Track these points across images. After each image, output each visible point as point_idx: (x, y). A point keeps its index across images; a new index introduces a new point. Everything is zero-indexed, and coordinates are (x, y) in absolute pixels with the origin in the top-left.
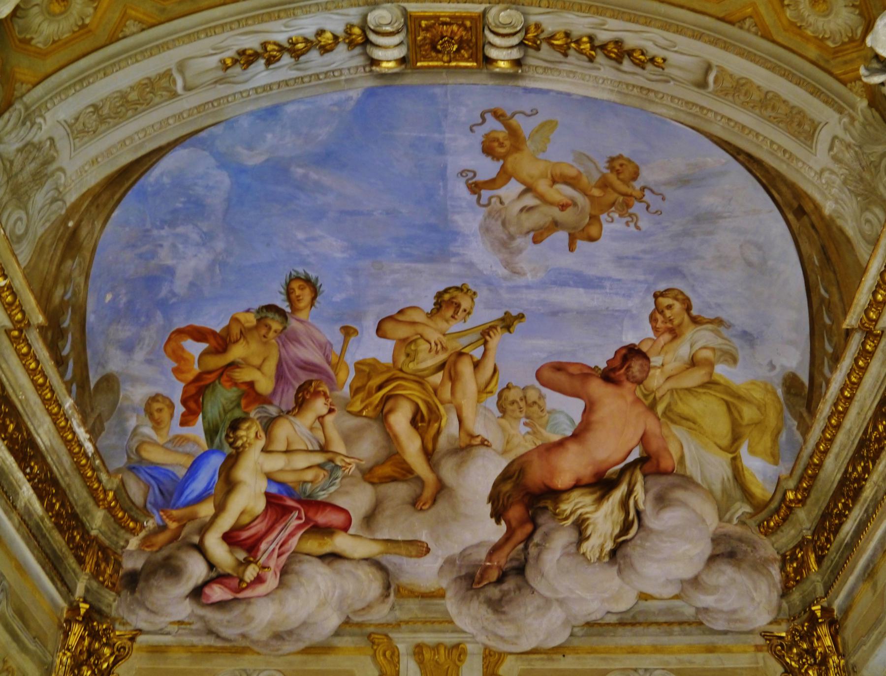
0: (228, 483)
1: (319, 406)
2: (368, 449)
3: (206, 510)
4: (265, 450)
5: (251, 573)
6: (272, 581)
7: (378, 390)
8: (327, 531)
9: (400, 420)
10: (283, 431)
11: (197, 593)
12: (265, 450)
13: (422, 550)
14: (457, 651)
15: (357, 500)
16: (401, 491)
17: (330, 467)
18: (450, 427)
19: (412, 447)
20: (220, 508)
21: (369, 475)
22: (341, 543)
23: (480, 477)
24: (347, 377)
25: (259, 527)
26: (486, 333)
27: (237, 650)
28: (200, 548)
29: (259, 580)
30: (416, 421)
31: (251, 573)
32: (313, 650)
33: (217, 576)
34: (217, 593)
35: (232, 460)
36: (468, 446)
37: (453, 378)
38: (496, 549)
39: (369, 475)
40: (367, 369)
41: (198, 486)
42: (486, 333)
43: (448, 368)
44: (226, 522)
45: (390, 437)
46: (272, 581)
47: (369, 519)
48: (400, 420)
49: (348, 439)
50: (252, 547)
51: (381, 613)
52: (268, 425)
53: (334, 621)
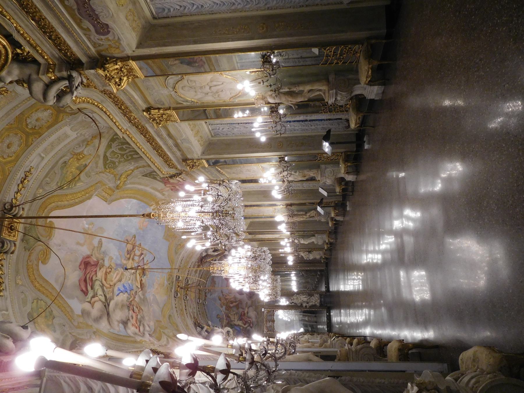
0: (239, 325)
1: (230, 315)
2: (235, 309)
3: (241, 328)
7: (228, 308)
8: (244, 314)
9: (231, 305)
10: (232, 319)
15: (241, 310)
16: (240, 305)
17: (237, 313)
18: (232, 299)
19: (234, 304)
20: (241, 326)
21: (238, 309)
22: (246, 312)
24: (227, 311)
26: (223, 295)
27: (258, 322)
30: (232, 303)
32: (258, 314)
33: (249, 325)
34: (251, 325)
35: (235, 325)
37: (227, 299)
39: (238, 309)
40: (226, 309)
41: (239, 329)
42: (223, 295)
43: (226, 299)
44: (243, 325)
45: (234, 306)
47: (243, 309)
48: (231, 305)
49: (233, 311)
50: (246, 322)
51: (254, 307)
52: (231, 321)
53: (255, 312)
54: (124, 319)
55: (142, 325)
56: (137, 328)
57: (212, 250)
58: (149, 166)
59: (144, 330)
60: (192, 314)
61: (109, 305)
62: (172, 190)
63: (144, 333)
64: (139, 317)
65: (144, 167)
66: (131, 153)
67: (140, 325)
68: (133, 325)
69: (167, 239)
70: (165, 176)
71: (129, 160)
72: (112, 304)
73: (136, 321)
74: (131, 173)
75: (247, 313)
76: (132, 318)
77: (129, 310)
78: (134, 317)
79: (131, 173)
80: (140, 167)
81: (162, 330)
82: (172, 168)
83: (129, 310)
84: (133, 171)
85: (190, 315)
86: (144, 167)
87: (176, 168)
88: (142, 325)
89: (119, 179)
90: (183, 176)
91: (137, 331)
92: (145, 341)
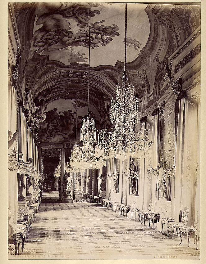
4: (51, 123)
5: (51, 136)
6: (53, 137)
11: (46, 138)
12: (51, 123)
13: (66, 134)
14: (69, 144)
19: (65, 123)
23: (72, 127)
25: (51, 131)
28: (46, 133)
29: (52, 136)
31: (51, 136)
34: (48, 138)
36: (71, 124)
38: (73, 134)
40: (61, 116)
46: (53, 137)
47: (62, 131)
48: (64, 121)
52: (52, 121)
54: (47, 28)
55: (44, 44)
56: (41, 39)
57: (109, 104)
58: (178, 47)
59: (40, 46)
60: (56, 86)
61: (58, 13)
62: (158, 68)
63: (37, 46)
64: (50, 41)
65: (178, 42)
66: (189, 30)
67: (43, 42)
68: (43, 36)
69: (117, 63)
70: (169, 63)
71: (184, 28)
72: (59, 17)
73: (47, 39)
74: (172, 30)
75: (58, 134)
76: (50, 35)
77: (55, 32)
78: (49, 37)
79: (172, 30)
80: (177, 38)
81: (41, 61)
82: (175, 69)
83: (55, 32)
84: (174, 32)
85: (56, 85)
86: (178, 42)
87: (175, 73)
88: (44, 44)
89: (167, 19)
90: (169, 79)
91: (39, 40)
92: (30, 47)
